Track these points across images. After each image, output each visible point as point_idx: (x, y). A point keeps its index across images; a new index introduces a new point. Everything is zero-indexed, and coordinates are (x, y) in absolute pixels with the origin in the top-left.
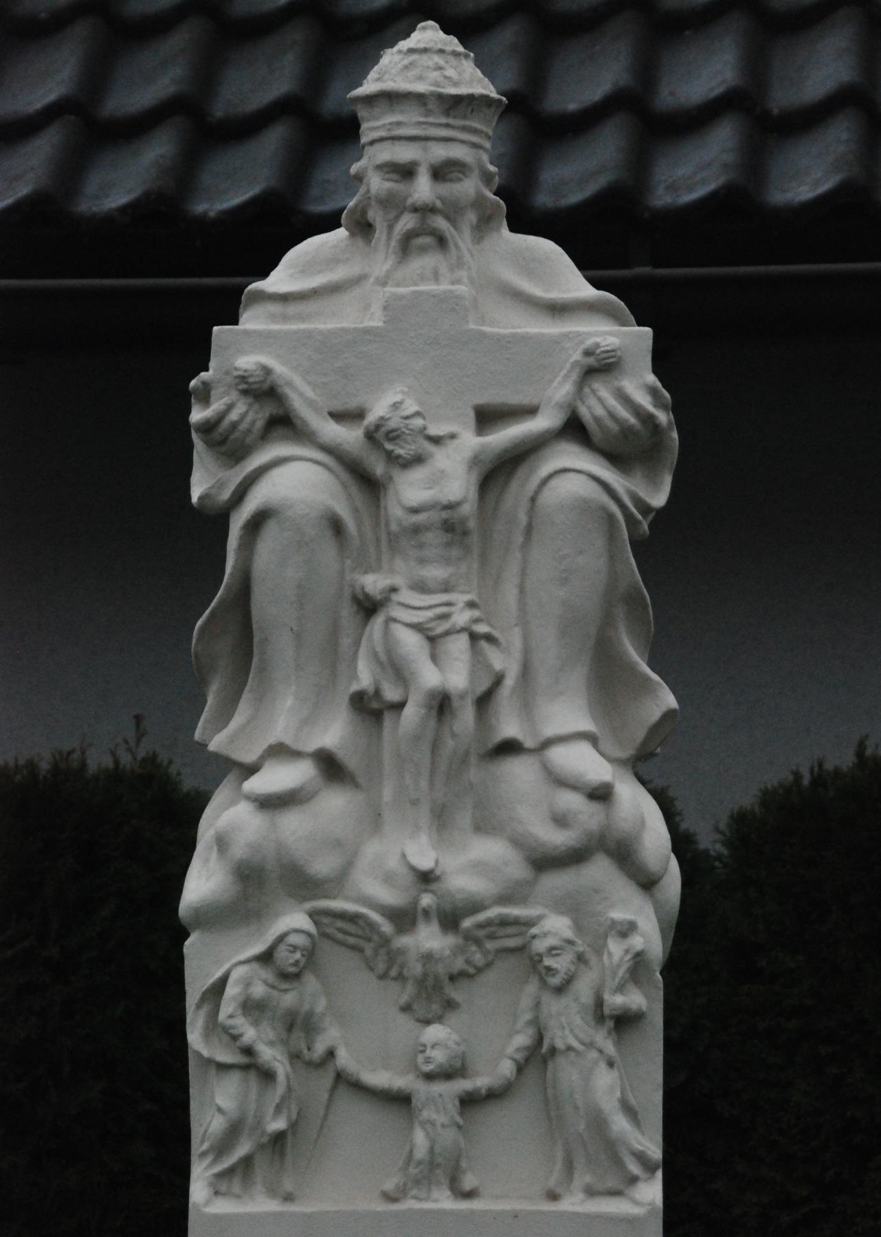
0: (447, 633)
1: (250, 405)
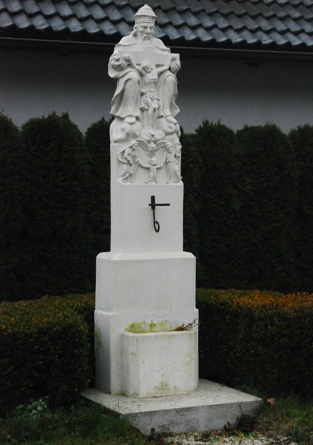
0: (154, 99)
1: (126, 62)
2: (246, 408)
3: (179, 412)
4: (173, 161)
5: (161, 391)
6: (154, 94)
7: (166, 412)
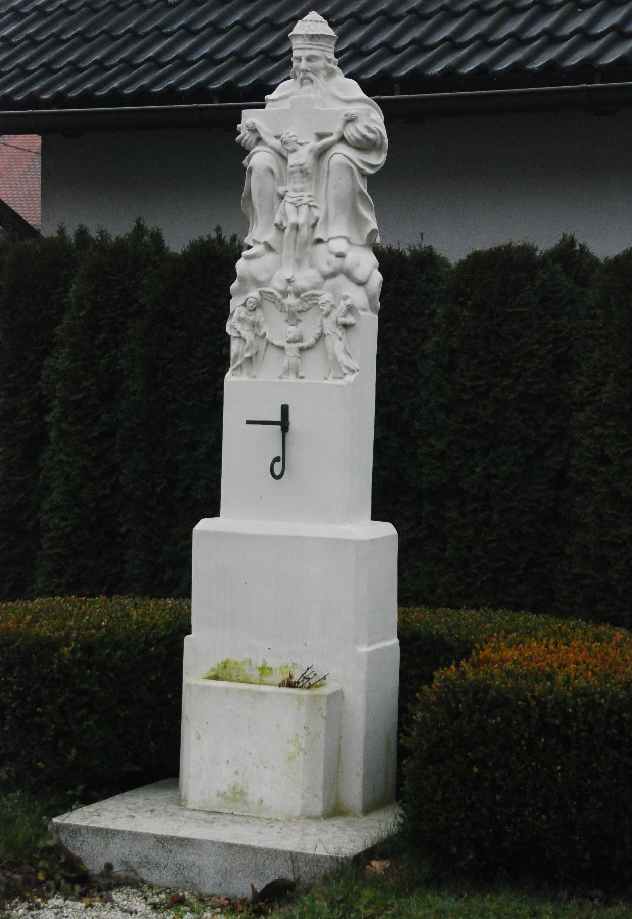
0: (301, 205)
1: (251, 134)
2: (308, 867)
3: (163, 842)
4: (332, 332)
5: (231, 804)
6: (302, 196)
7: (136, 836)
